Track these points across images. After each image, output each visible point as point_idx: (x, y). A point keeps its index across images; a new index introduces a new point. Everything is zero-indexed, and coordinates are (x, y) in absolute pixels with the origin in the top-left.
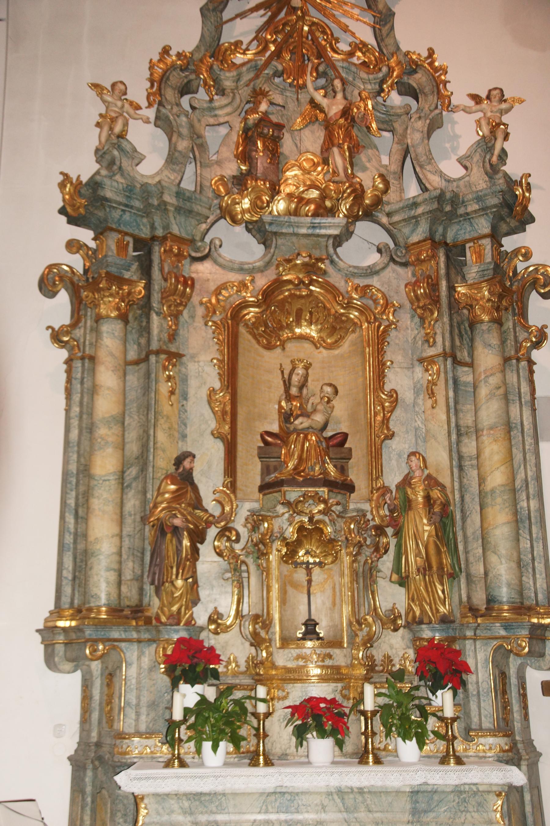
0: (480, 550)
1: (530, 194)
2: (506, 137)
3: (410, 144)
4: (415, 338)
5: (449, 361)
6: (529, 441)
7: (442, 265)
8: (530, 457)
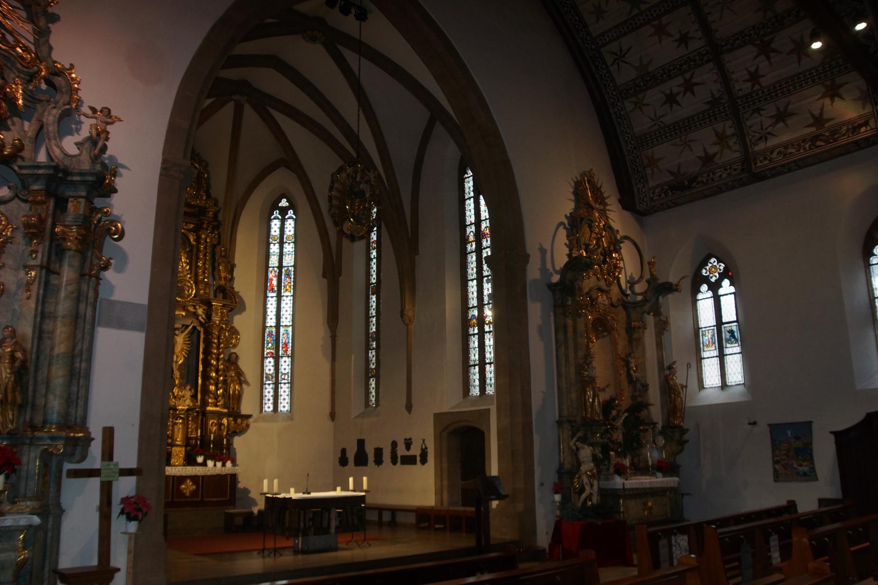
0: (44, 390)
1: (115, 178)
2: (107, 139)
3: (45, 123)
4: (23, 251)
5: (44, 271)
6: (88, 326)
7: (51, 208)
8: (87, 337)
